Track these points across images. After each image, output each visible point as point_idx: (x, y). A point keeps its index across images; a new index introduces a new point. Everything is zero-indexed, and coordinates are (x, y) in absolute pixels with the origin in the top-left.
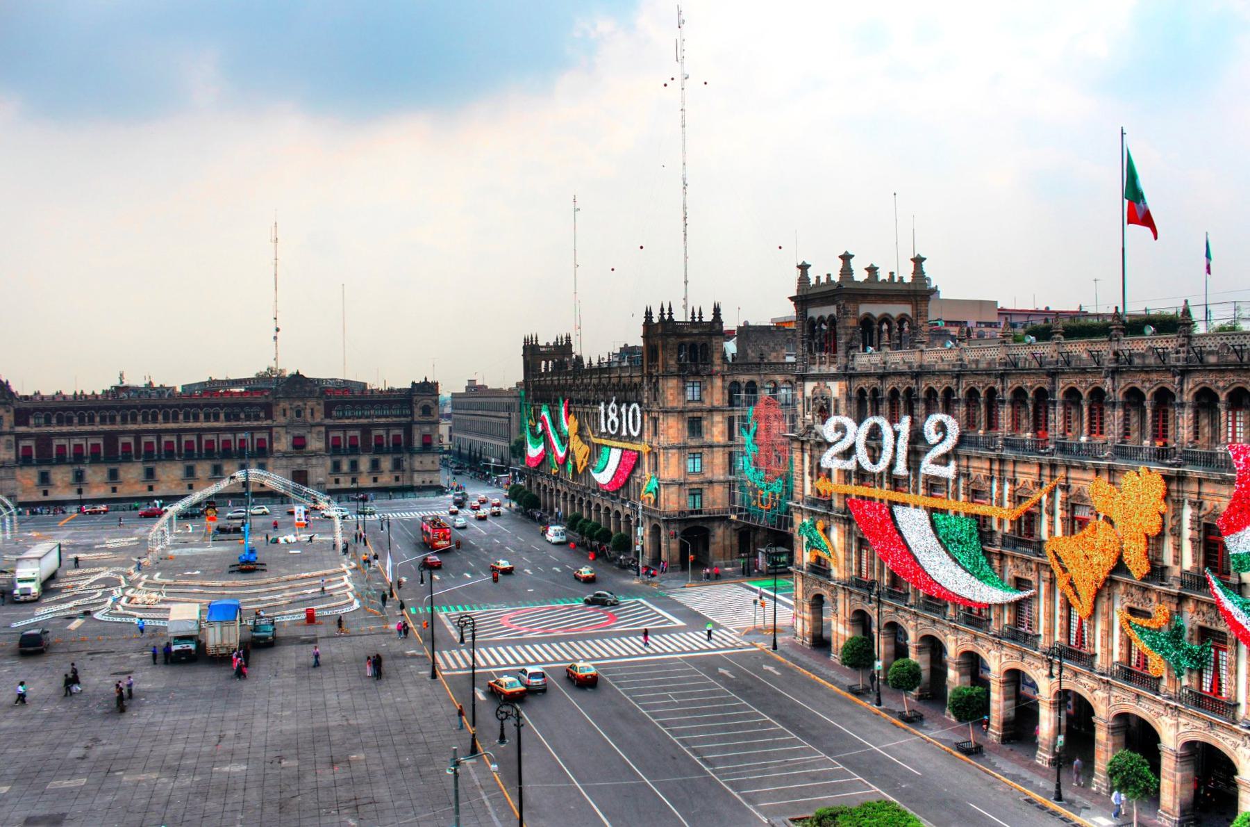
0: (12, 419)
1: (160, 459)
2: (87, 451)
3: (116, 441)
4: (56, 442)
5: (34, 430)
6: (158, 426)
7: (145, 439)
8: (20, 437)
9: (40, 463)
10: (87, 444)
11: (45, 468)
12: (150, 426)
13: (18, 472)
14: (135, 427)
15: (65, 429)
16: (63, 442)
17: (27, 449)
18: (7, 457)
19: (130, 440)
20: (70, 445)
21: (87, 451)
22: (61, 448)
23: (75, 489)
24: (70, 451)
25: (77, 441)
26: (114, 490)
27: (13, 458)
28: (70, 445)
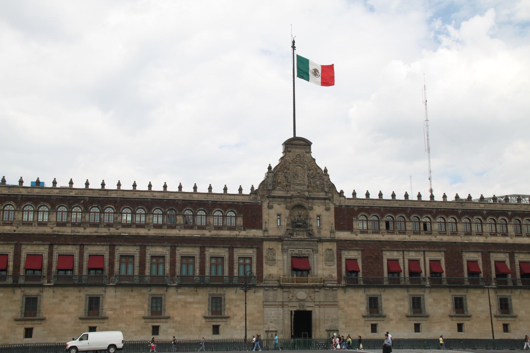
0: (332, 219)
1: (515, 287)
2: (425, 271)
3: (461, 257)
4: (387, 255)
5: (360, 237)
6: (509, 240)
7: (496, 257)
8: (343, 245)
9: (368, 284)
10: (425, 260)
11: (373, 292)
12: (500, 239)
13: (340, 295)
14: (481, 240)
15: (397, 237)
16: (395, 255)
17: (351, 262)
18: (326, 273)
19: (476, 257)
20: (404, 259)
21: (425, 271)
22: (393, 263)
23: (411, 325)
24: (404, 267)
25: (413, 255)
26: (460, 328)
27: (335, 275)
28: (404, 259)
